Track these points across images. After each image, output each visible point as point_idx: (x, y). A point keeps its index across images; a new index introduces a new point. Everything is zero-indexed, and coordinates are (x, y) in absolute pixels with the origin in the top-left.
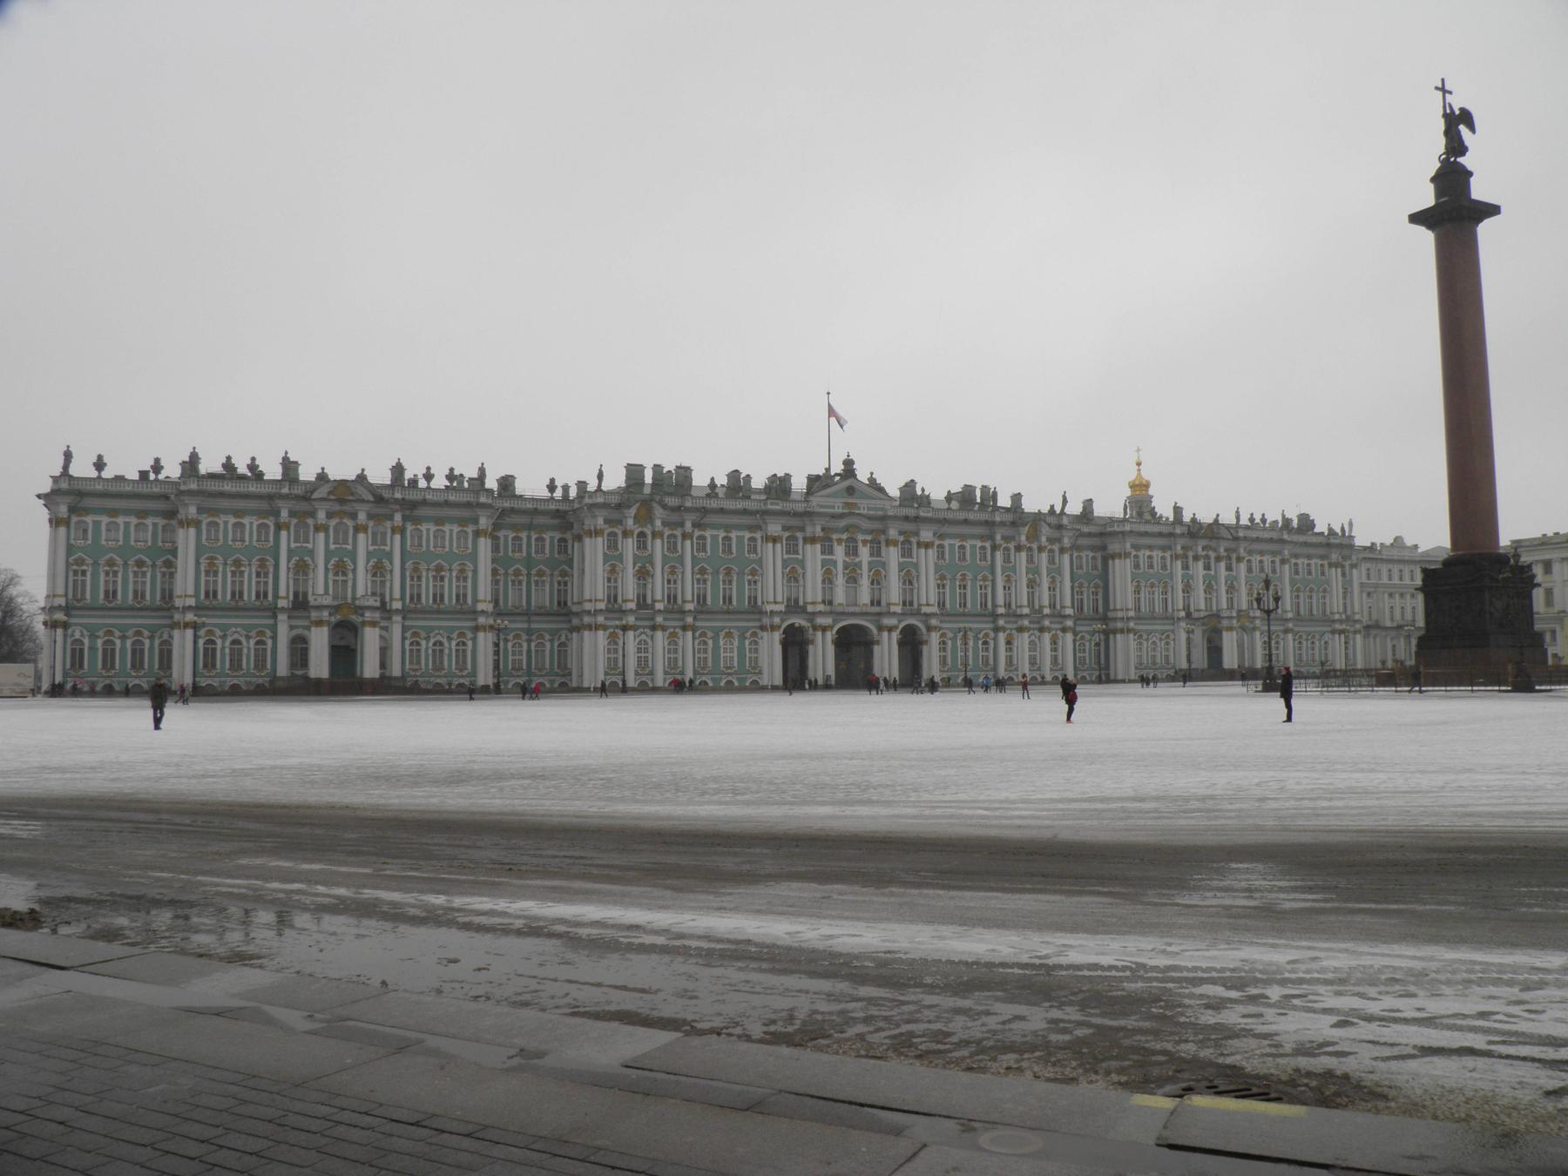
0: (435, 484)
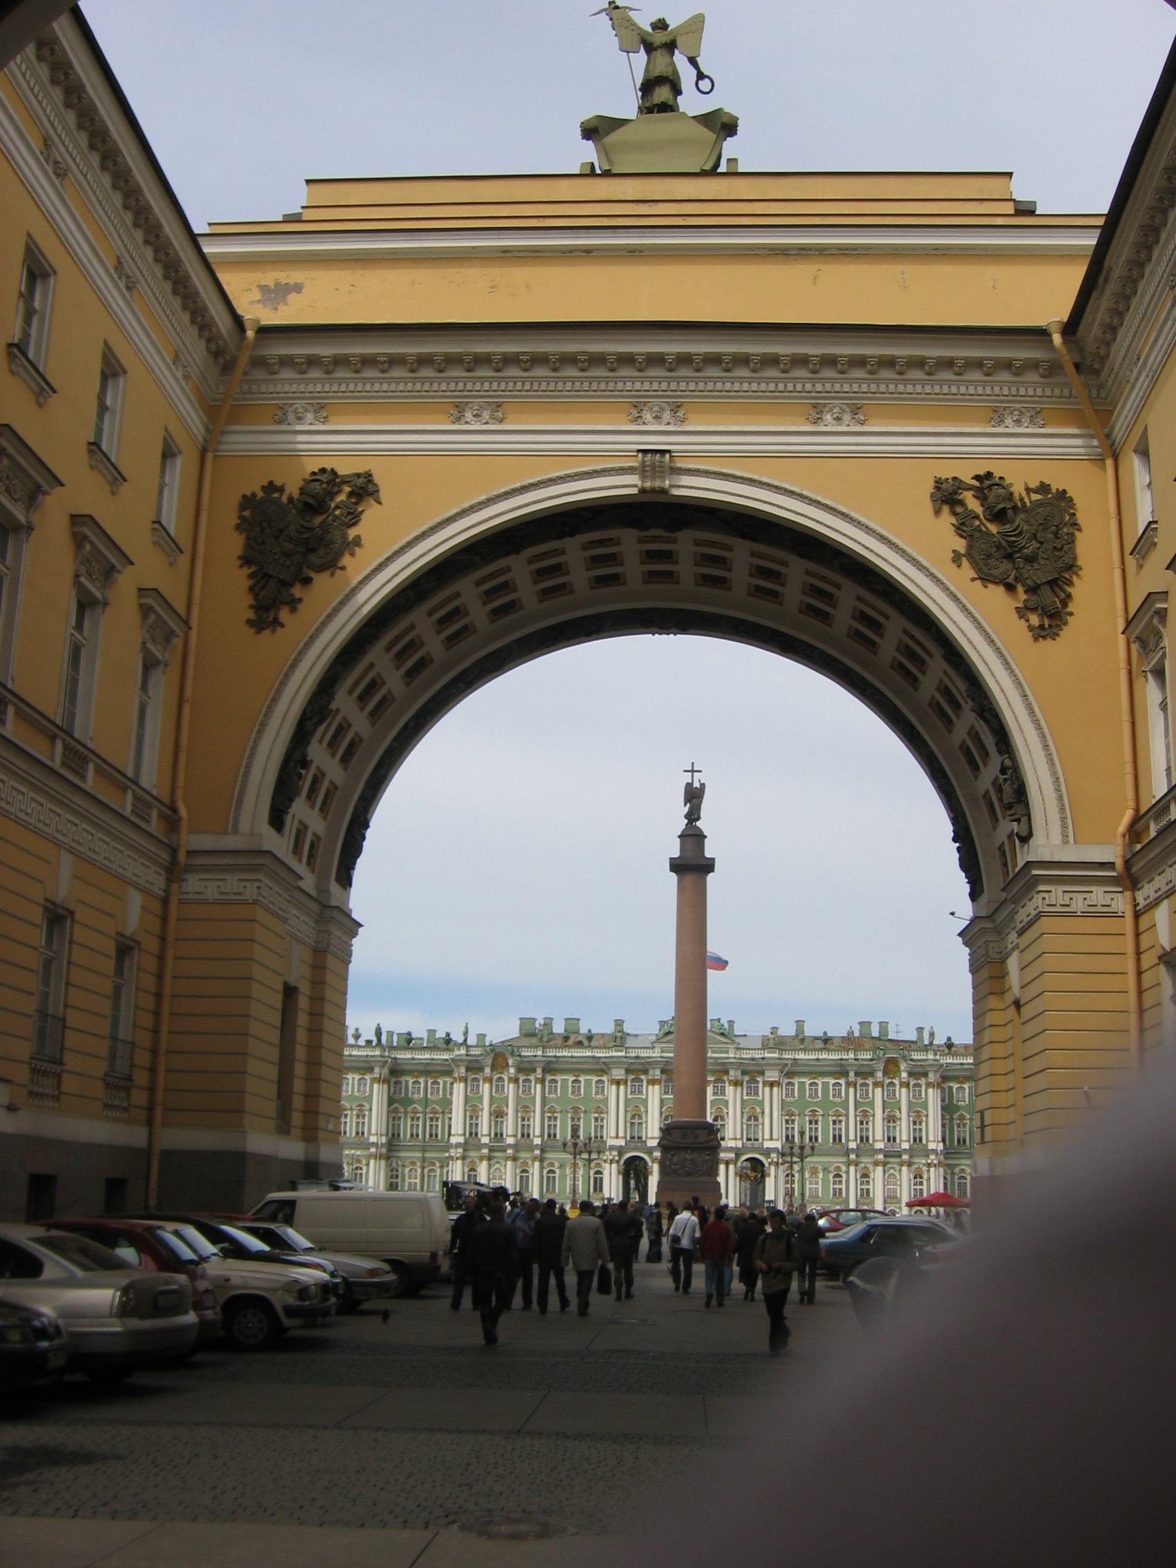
0: (361, 1042)
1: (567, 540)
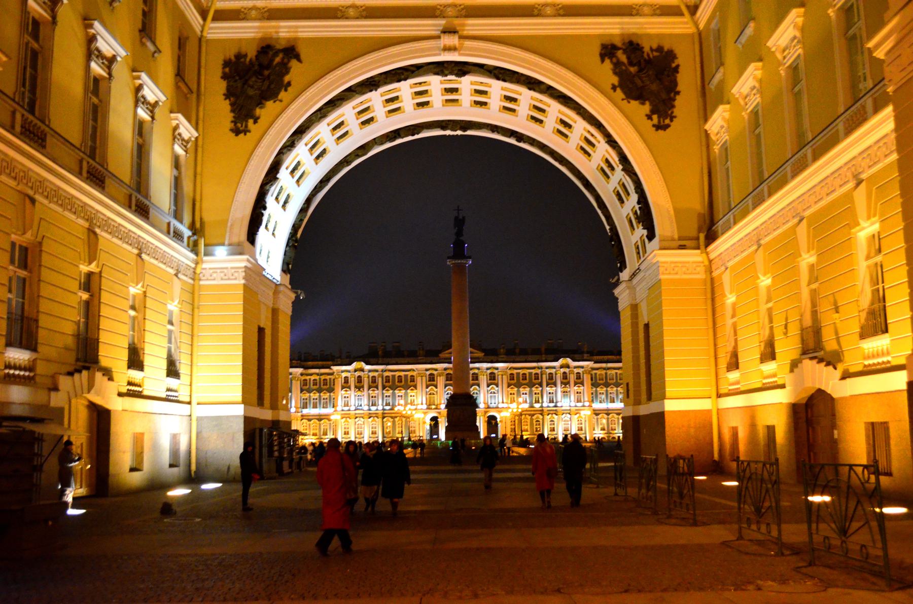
1: (403, 82)
